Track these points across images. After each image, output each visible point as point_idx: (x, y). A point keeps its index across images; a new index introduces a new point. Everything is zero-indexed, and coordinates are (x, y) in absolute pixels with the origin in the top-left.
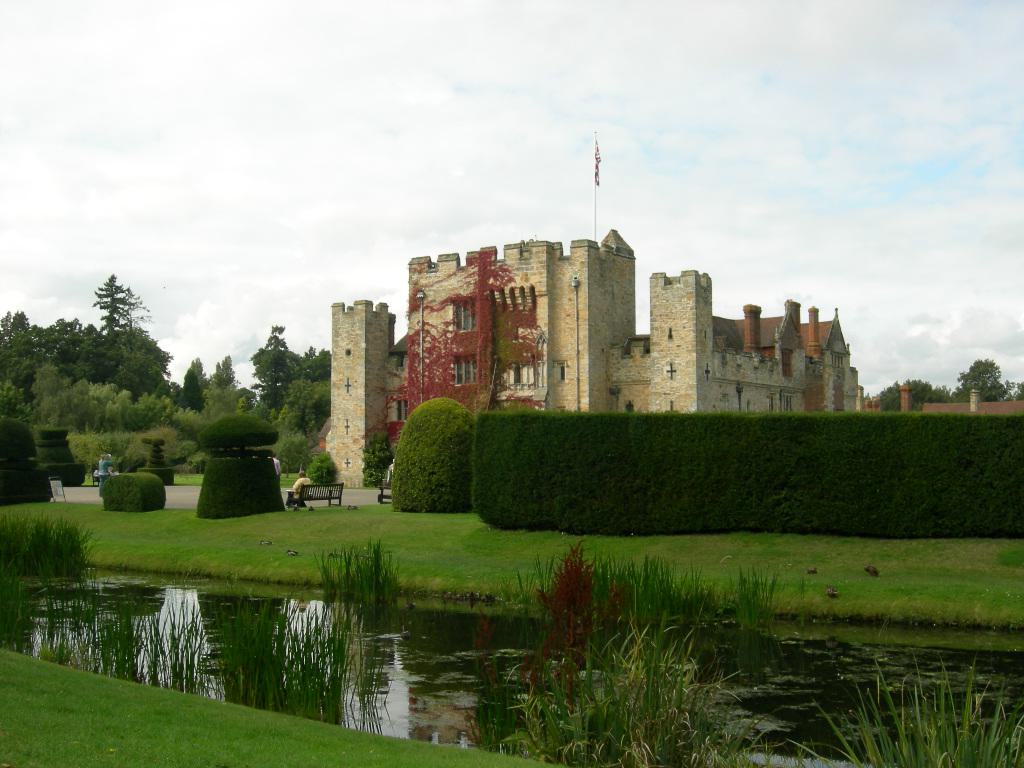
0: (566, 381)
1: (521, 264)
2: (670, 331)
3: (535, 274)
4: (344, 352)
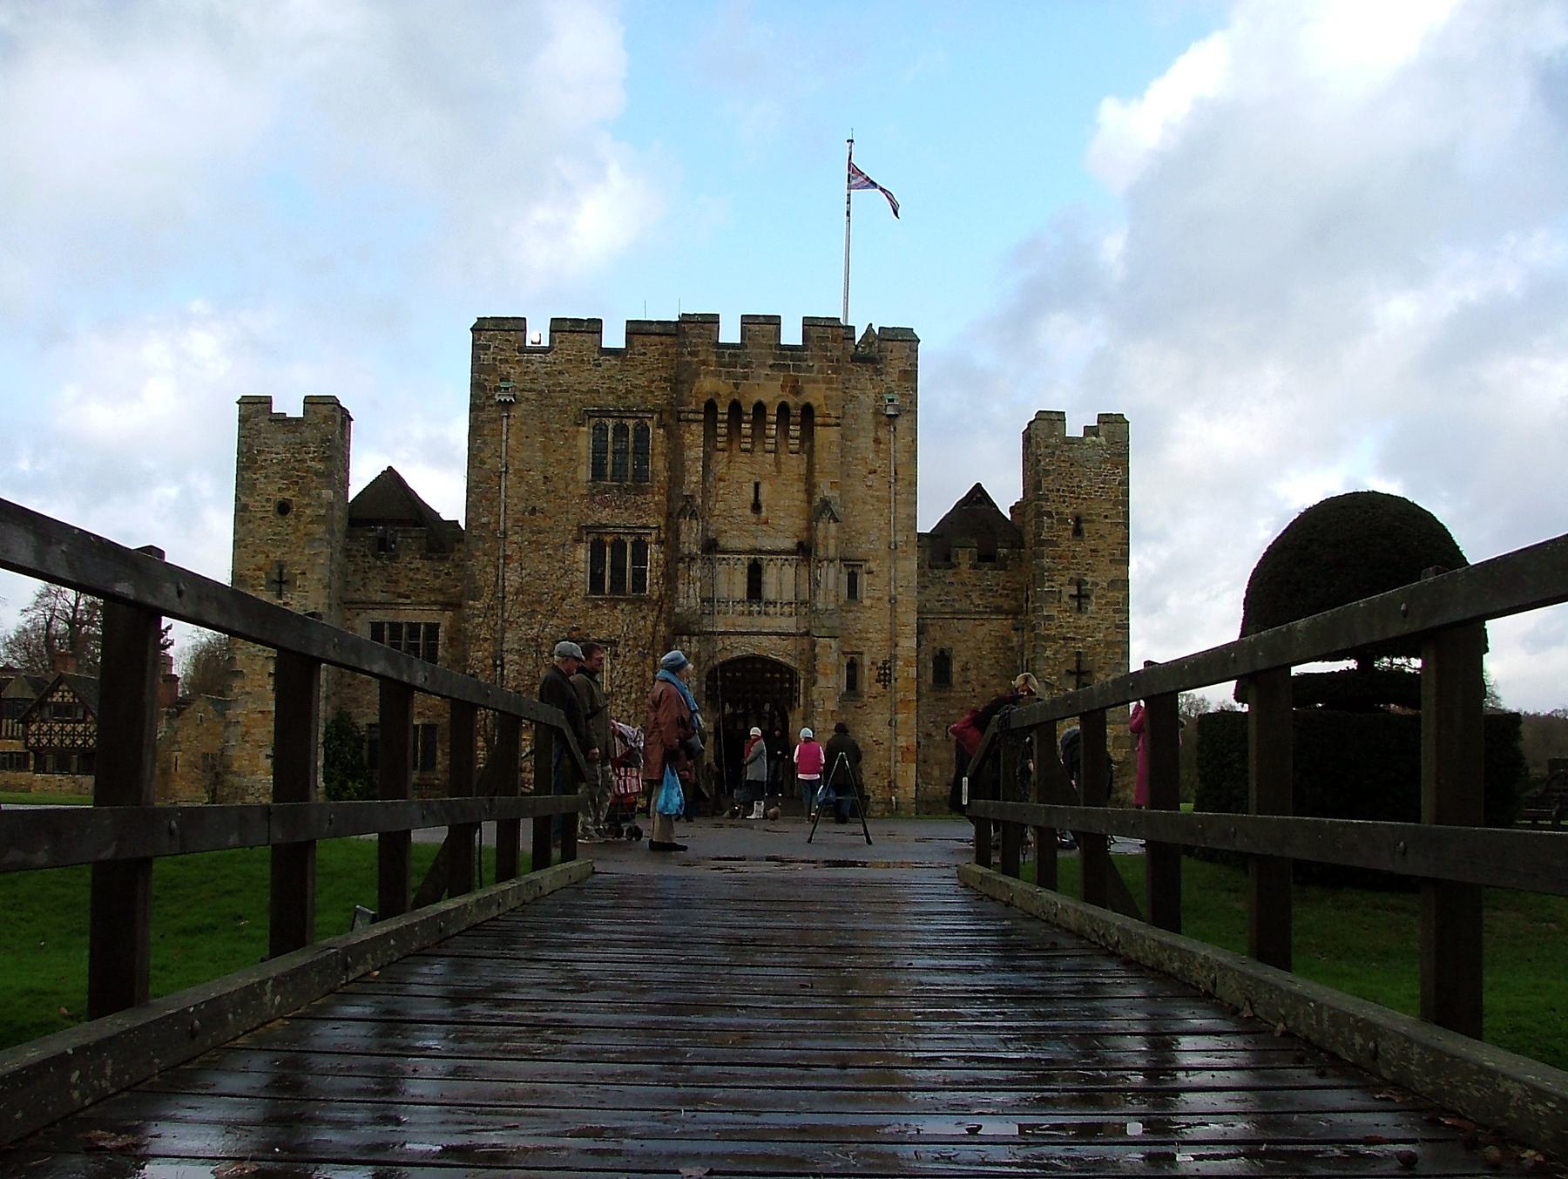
0: (867, 602)
1: (785, 358)
3: (815, 381)
4: (271, 507)
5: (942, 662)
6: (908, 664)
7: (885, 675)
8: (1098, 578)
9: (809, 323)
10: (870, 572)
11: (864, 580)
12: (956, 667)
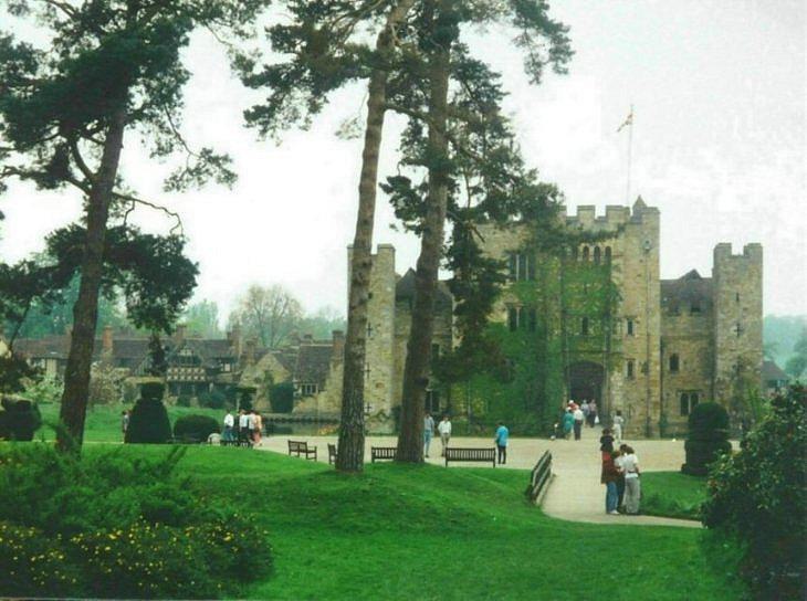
2: (738, 294)
5: (674, 361)
6: (656, 364)
7: (646, 369)
8: (748, 320)
9: (609, 208)
10: (638, 322)
11: (635, 326)
12: (681, 362)
